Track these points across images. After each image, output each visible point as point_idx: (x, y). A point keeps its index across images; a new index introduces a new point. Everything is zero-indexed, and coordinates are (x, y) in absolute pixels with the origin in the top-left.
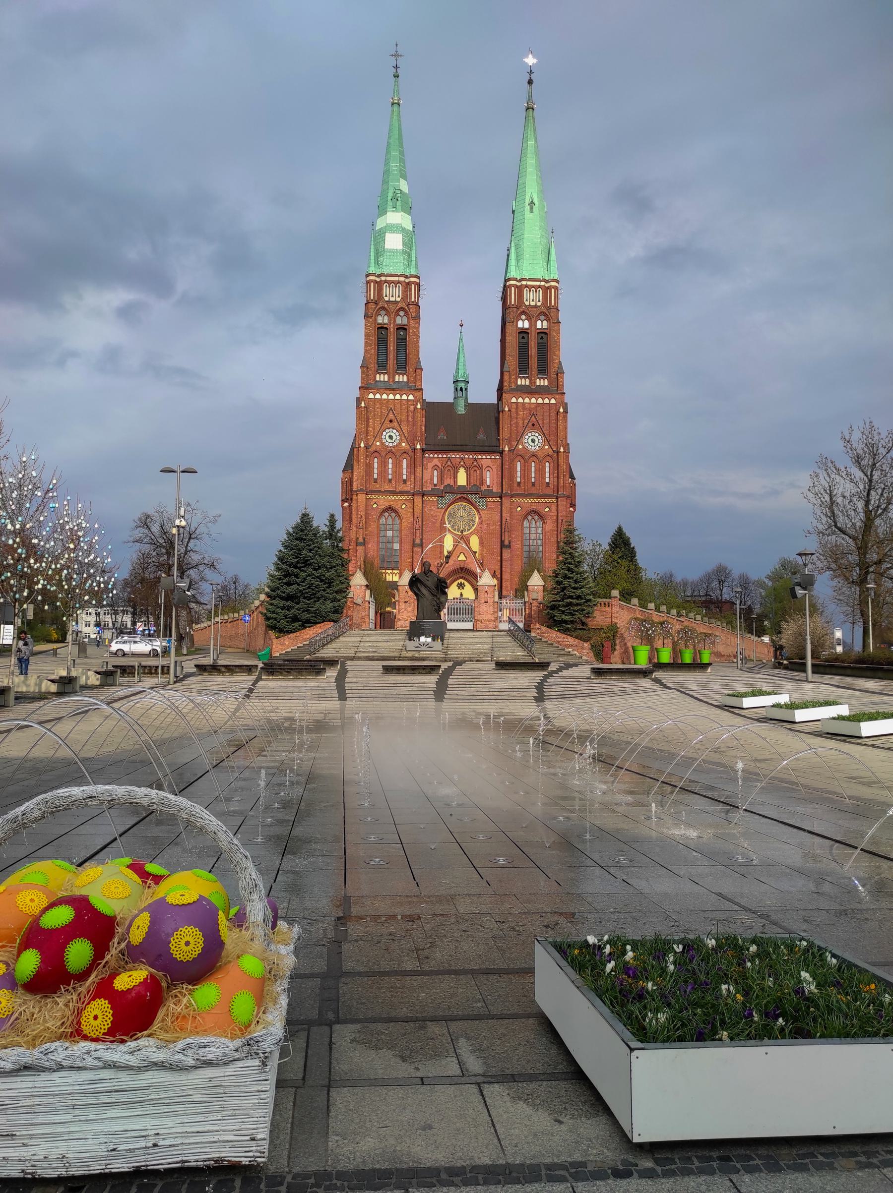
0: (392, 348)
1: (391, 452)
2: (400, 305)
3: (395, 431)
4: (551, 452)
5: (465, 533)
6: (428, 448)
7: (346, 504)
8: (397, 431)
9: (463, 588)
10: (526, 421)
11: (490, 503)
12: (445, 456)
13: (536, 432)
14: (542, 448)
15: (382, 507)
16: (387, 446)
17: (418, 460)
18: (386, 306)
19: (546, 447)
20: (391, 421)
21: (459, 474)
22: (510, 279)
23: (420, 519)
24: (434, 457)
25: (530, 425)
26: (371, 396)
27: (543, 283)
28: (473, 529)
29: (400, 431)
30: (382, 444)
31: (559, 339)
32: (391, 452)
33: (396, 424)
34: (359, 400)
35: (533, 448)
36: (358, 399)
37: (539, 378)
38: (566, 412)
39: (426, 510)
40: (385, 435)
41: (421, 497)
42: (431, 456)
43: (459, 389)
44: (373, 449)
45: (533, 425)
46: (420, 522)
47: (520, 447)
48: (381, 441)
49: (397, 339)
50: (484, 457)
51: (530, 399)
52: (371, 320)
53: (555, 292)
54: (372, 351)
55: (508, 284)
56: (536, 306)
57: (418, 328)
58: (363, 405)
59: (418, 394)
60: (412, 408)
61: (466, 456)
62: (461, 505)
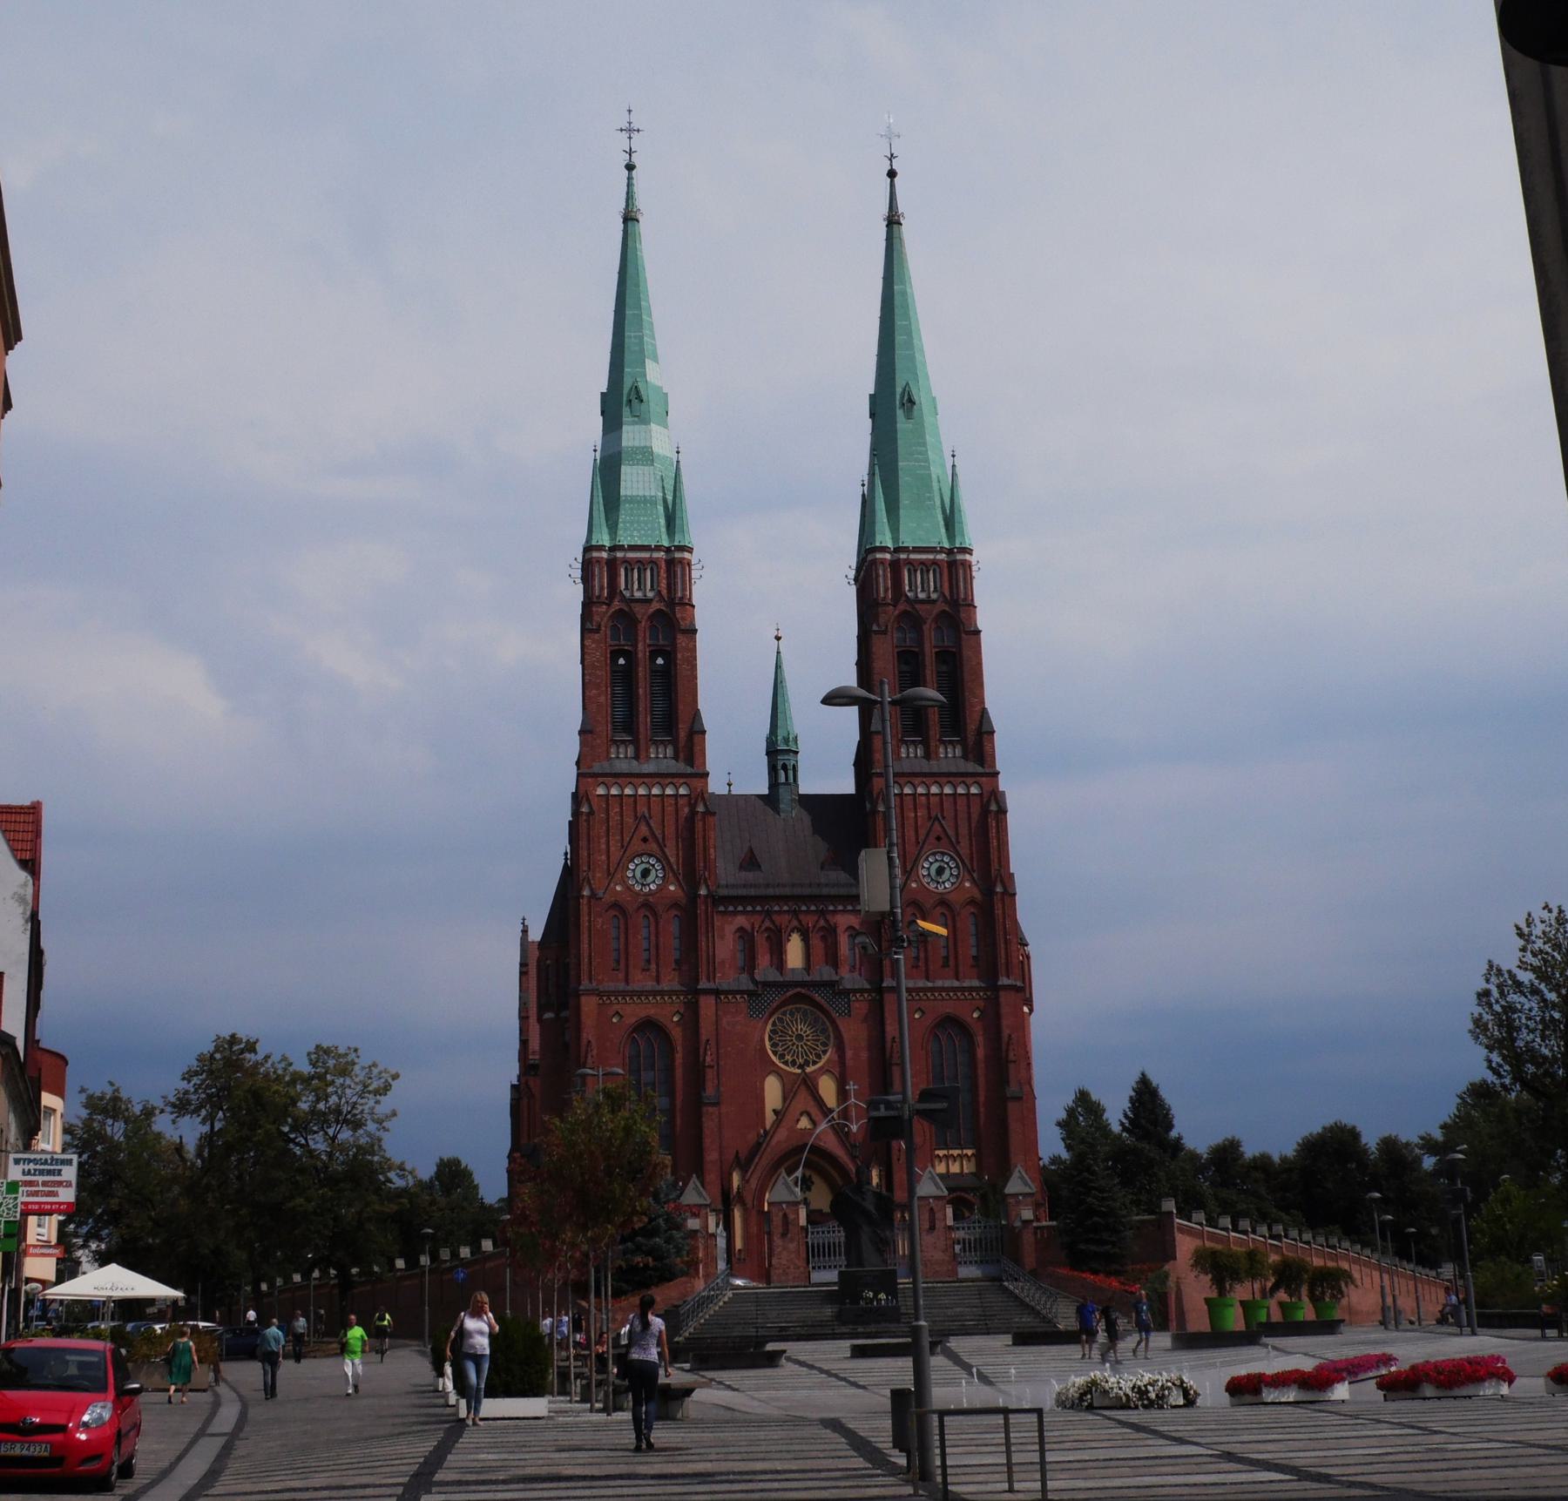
0: (641, 691)
1: (646, 905)
2: (656, 606)
4: (977, 895)
5: (809, 1070)
7: (548, 1015)
8: (658, 860)
9: (809, 1189)
10: (923, 833)
11: (857, 1005)
13: (943, 854)
14: (958, 888)
15: (633, 1020)
16: (638, 894)
17: (701, 921)
18: (626, 609)
19: (967, 884)
20: (645, 840)
23: (713, 1042)
25: (932, 839)
28: (825, 1059)
29: (663, 859)
30: (629, 888)
31: (980, 664)
32: (648, 905)
33: (654, 846)
34: (576, 797)
35: (941, 888)
36: (575, 796)
37: (944, 742)
38: (1002, 811)
39: (724, 1021)
40: (635, 868)
41: (713, 997)
42: (731, 908)
44: (608, 898)
45: (938, 839)
46: (714, 1050)
48: (623, 881)
49: (652, 671)
50: (840, 908)
52: (597, 636)
53: (965, 571)
54: (602, 699)
55: (870, 557)
56: (928, 601)
57: (694, 649)
58: (585, 809)
59: (696, 783)
61: (804, 908)
62: (798, 1010)
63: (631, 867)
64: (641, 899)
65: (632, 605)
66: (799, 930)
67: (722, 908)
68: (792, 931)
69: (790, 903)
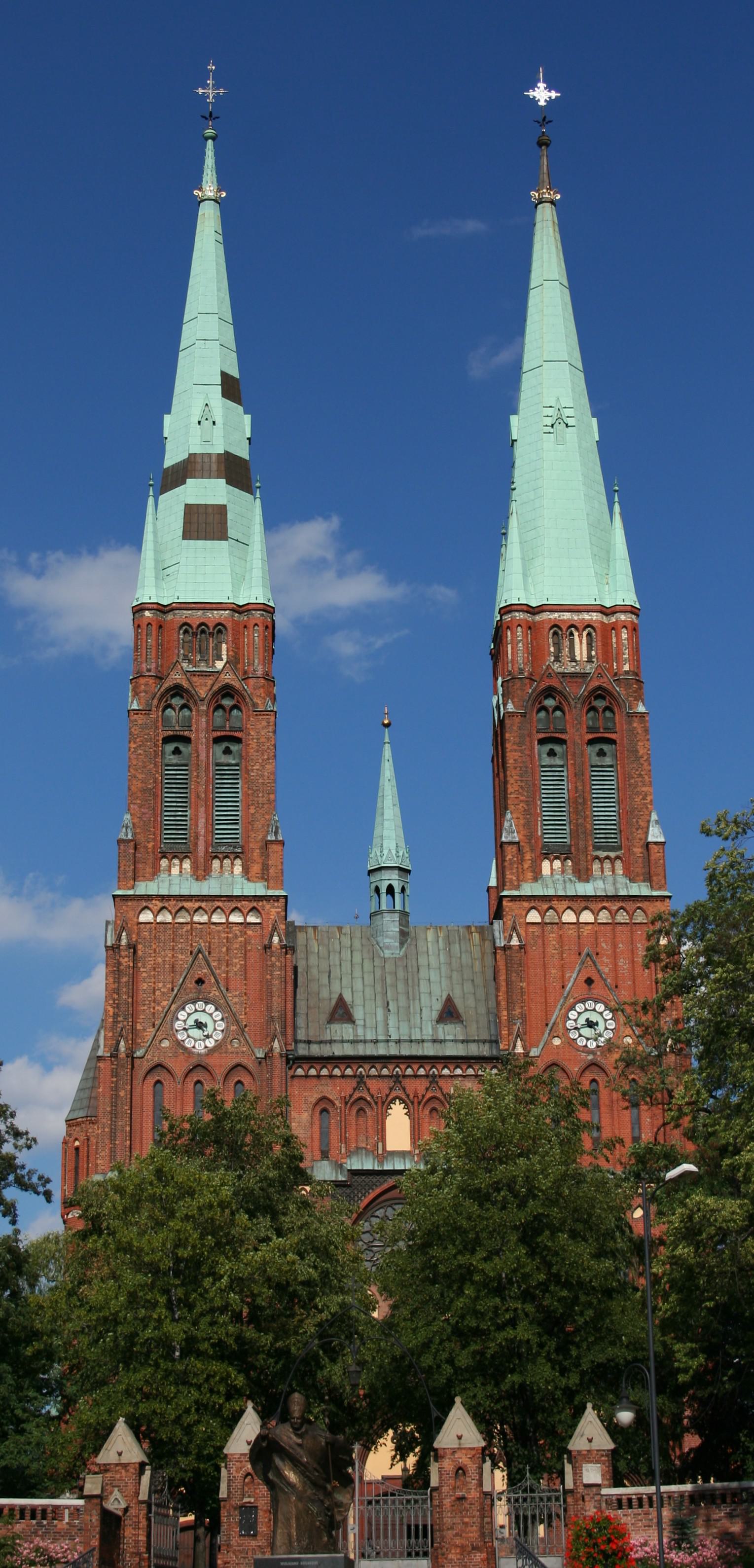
3: (210, 1008)
6: (302, 1050)
12: (349, 1072)
13: (596, 1001)
18: (185, 684)
20: (200, 981)
21: (389, 1121)
22: (508, 609)
24: (318, 1076)
26: (146, 917)
27: (595, 616)
43: (383, 890)
47: (557, 1042)
48: (171, 1034)
51: (578, 915)
60: (256, 945)
63: (180, 1017)
64: (194, 1061)
65: (195, 679)
66: (402, 1101)
67: (300, 1072)
68: (393, 1101)
69: (391, 1067)
